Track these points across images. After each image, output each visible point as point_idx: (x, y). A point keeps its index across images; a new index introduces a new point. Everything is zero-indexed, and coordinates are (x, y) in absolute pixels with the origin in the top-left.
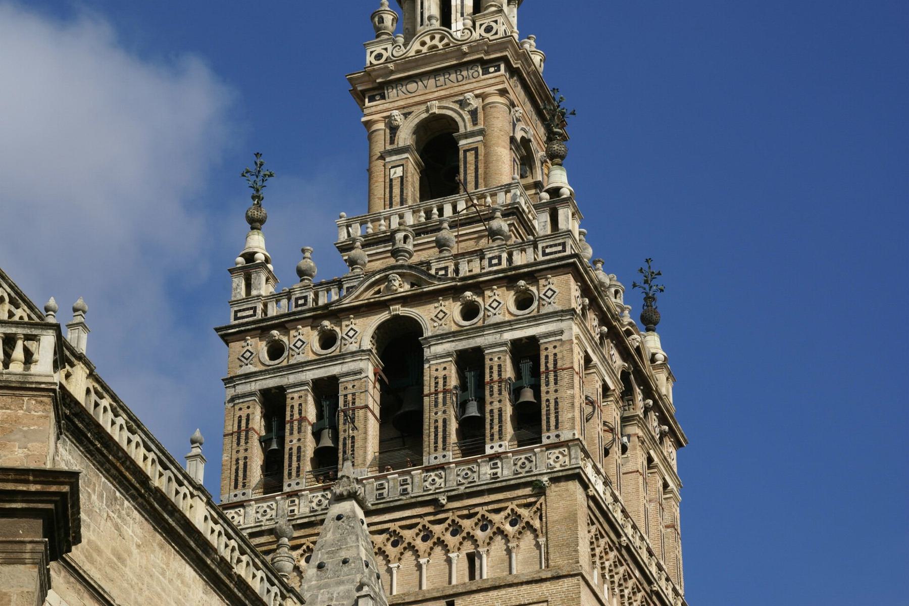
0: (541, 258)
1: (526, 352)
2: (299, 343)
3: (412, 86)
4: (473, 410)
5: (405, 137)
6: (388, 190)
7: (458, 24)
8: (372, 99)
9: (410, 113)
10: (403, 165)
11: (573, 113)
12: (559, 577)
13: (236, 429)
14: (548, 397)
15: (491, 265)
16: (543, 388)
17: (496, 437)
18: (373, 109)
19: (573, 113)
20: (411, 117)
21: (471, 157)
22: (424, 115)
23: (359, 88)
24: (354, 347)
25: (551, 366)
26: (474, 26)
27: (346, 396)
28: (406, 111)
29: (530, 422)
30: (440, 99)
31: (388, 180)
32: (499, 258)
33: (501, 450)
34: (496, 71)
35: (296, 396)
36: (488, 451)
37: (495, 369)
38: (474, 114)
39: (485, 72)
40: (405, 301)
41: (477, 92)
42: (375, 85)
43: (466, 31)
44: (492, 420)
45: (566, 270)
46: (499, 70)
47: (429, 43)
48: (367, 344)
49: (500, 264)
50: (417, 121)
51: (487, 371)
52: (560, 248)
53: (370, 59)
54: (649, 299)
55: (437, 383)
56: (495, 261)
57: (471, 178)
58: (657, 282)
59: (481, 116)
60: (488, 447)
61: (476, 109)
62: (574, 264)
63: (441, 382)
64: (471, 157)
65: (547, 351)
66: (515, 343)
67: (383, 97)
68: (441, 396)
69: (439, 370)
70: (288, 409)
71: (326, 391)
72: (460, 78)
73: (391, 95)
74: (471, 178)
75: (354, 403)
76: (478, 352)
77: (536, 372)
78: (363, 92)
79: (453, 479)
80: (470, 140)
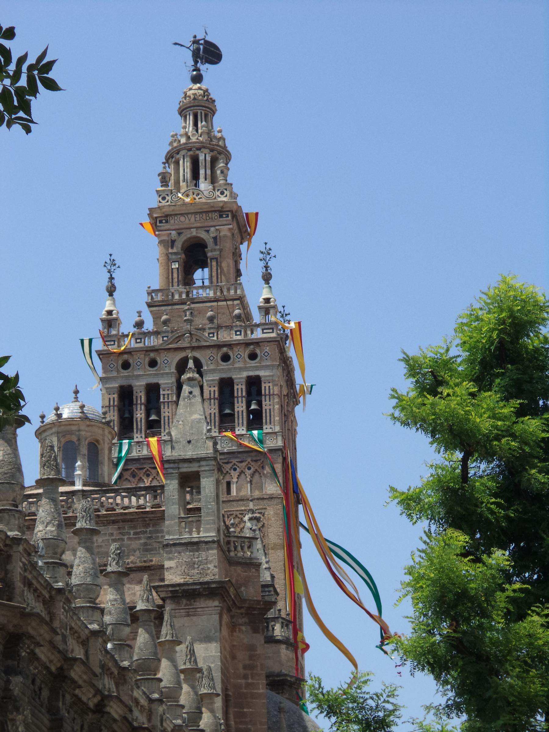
2: (139, 363)
3: (182, 219)
6: (170, 275)
7: (204, 185)
8: (161, 222)
9: (181, 233)
10: (178, 261)
11: (275, 257)
12: (272, 498)
13: (108, 404)
14: (266, 407)
15: (236, 335)
16: (264, 403)
17: (240, 425)
18: (162, 228)
19: (275, 257)
20: (182, 236)
22: (189, 236)
23: (155, 215)
25: (267, 392)
26: (214, 190)
27: (164, 395)
28: (179, 231)
29: (256, 420)
30: (197, 228)
31: (170, 269)
32: (240, 331)
33: (244, 432)
34: (226, 217)
35: (138, 391)
37: (240, 390)
38: (215, 238)
39: (221, 216)
40: (193, 348)
41: (217, 227)
42: (163, 215)
43: (211, 193)
44: (238, 416)
45: (274, 343)
46: (228, 216)
49: (240, 334)
50: (185, 238)
51: (236, 391)
52: (271, 331)
55: (210, 394)
56: (238, 333)
59: (218, 240)
60: (236, 430)
61: (216, 236)
62: (278, 341)
63: (212, 394)
66: (249, 378)
67: (167, 222)
68: (212, 401)
70: (134, 398)
72: (208, 218)
73: (172, 221)
75: (168, 399)
77: (259, 393)
78: (156, 218)
80: (214, 253)
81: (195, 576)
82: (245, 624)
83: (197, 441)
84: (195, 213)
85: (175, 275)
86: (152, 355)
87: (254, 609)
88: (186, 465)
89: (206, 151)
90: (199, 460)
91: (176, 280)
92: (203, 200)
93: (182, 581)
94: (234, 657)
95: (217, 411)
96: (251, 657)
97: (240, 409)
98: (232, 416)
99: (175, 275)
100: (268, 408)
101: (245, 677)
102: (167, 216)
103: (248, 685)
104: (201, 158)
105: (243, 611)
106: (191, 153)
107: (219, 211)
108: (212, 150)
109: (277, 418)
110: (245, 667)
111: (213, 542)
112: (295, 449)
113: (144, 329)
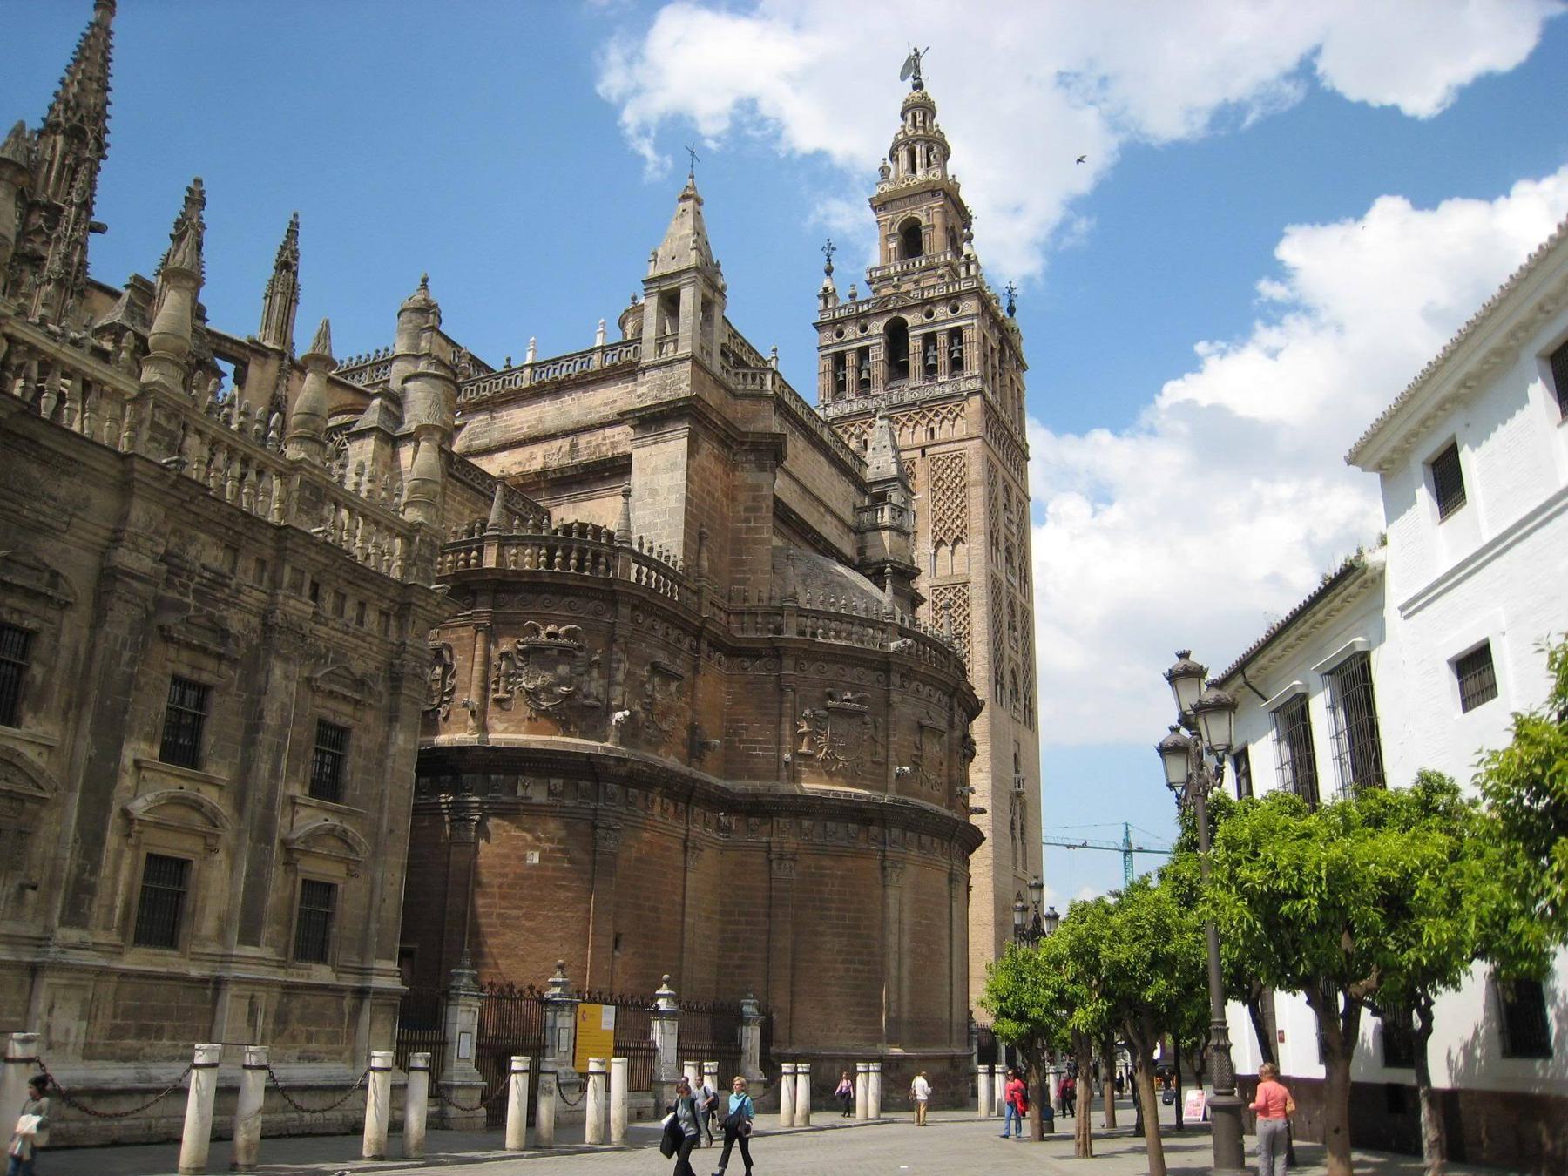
1: (956, 334)
4: (931, 362)
5: (896, 229)
7: (920, 172)
40: (899, 310)
54: (1011, 301)
65: (966, 333)
69: (915, 344)
71: (863, 353)
76: (934, 334)
77: (960, 343)
79: (924, 394)
94: (734, 499)
96: (754, 499)
101: (747, 520)
103: (749, 529)
110: (746, 510)
111: (686, 359)
112: (1021, 408)
113: (858, 299)
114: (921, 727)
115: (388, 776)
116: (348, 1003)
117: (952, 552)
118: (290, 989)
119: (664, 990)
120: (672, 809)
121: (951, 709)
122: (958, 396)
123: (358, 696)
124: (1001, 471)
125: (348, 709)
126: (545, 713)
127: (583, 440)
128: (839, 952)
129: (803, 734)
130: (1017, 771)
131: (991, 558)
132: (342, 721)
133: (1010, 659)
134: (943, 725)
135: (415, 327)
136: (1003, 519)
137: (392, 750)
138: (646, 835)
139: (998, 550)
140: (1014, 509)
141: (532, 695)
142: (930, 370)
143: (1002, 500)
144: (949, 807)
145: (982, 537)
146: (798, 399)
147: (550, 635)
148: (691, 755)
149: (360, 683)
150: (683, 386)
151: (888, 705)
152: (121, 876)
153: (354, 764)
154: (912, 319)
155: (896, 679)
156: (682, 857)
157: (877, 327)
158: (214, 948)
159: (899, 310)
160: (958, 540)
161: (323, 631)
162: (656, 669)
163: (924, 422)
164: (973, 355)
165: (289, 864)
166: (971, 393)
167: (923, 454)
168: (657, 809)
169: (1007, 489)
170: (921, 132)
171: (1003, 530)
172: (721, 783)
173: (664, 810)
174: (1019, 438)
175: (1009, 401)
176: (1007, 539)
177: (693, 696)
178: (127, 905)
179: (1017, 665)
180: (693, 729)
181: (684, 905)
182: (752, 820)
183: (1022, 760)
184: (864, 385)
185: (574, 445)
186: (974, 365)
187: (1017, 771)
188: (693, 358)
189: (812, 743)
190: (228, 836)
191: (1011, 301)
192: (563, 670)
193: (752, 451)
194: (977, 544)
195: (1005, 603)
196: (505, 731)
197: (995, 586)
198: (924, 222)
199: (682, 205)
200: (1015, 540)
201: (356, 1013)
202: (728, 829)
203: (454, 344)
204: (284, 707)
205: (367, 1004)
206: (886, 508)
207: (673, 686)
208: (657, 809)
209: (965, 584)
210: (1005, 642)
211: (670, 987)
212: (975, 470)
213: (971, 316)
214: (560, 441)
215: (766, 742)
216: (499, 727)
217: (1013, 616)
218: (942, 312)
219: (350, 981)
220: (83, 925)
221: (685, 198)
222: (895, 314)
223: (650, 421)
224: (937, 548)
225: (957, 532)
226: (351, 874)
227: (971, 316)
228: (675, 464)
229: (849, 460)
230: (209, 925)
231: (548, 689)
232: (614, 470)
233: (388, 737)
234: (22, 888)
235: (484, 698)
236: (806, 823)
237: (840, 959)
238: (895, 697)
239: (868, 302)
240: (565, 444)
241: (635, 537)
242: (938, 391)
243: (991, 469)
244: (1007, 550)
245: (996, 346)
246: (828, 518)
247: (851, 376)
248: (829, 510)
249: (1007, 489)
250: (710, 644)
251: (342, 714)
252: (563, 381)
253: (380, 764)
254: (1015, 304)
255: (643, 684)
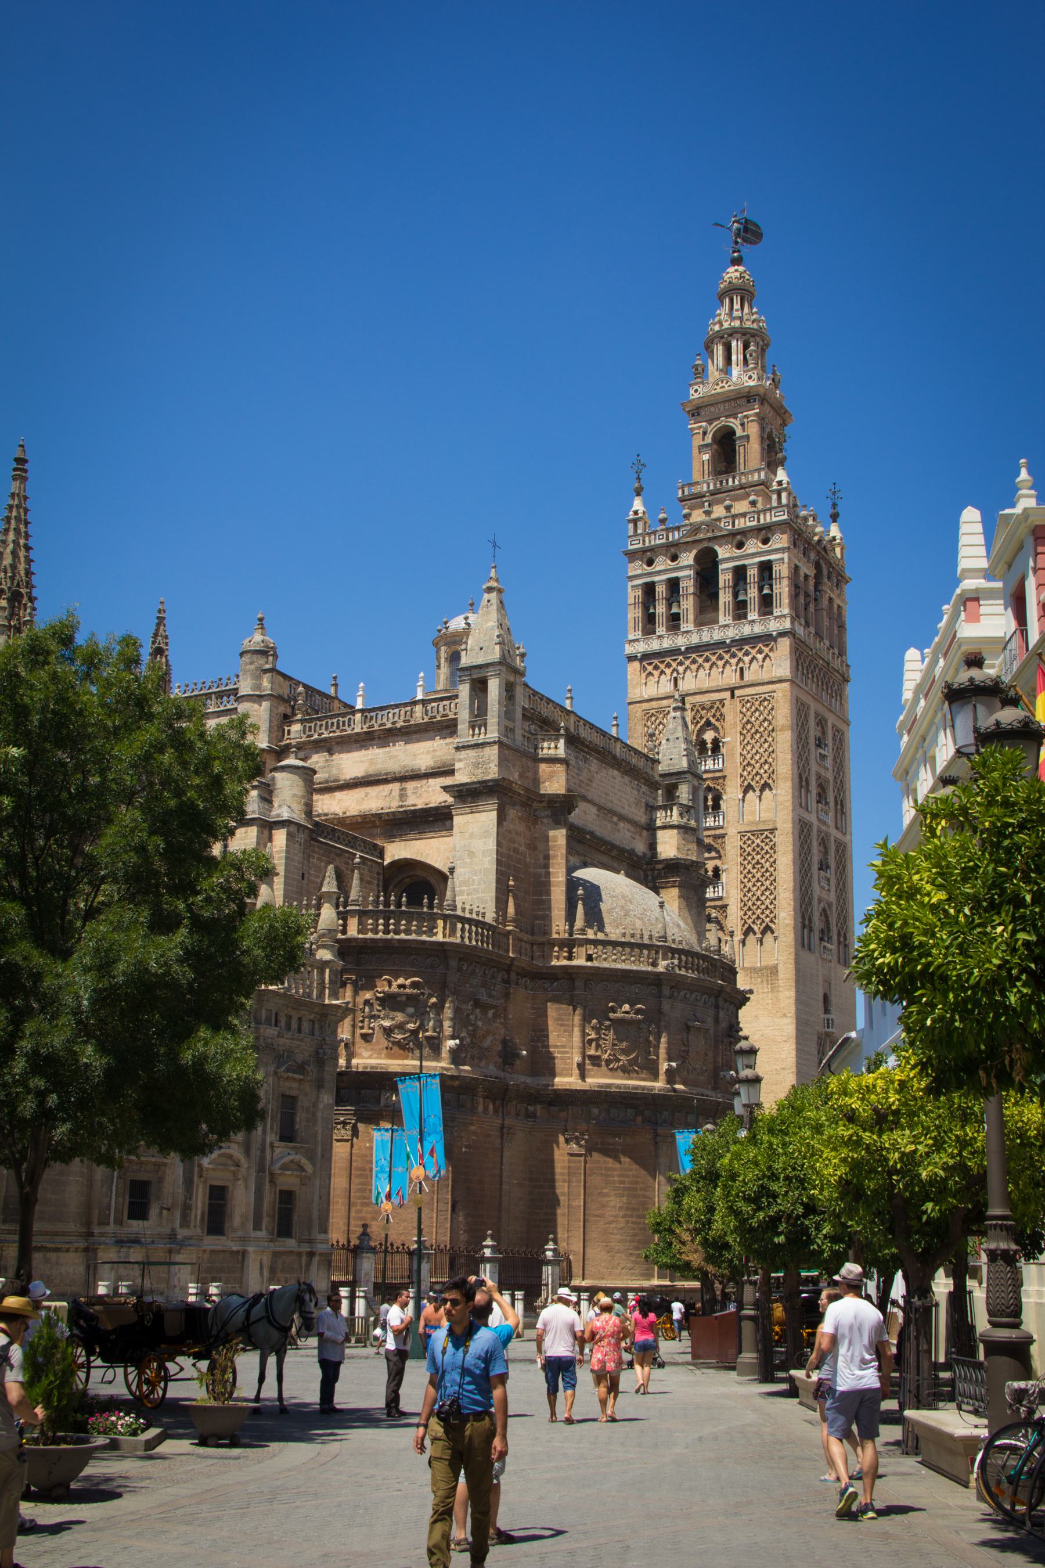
0: (774, 519)
3: (712, 409)
5: (709, 439)
21: (742, 450)
24: (686, 563)
36: (749, 618)
39: (749, 402)
47: (721, 385)
48: (691, 562)
53: (692, 392)
54: (834, 506)
57: (742, 461)
58: (838, 495)
64: (742, 450)
65: (776, 568)
66: (761, 563)
69: (725, 578)
74: (742, 461)
77: (771, 578)
81: (480, 776)
82: (548, 816)
83: (488, 648)
84: (724, 402)
85: (706, 467)
86: (672, 550)
87: (556, 802)
88: (477, 671)
89: (739, 335)
90: (487, 665)
91: (706, 472)
92: (732, 388)
93: (468, 781)
94: (535, 849)
95: (731, 599)
97: (752, 595)
98: (745, 602)
99: (706, 467)
100: (778, 591)
102: (698, 408)
104: (734, 344)
105: (544, 804)
106: (723, 340)
107: (747, 397)
108: (744, 334)
109: (787, 601)
111: (495, 742)
112: (842, 627)
114: (688, 1028)
115: (319, 1123)
116: (304, 1259)
117: (760, 797)
118: (276, 1255)
119: (489, 1242)
120: (491, 1107)
121: (717, 1007)
122: (767, 639)
123: (301, 1077)
124: (813, 706)
125: (295, 1085)
126: (397, 1044)
127: (410, 785)
128: (621, 1208)
129: (590, 1041)
130: (827, 1011)
131: (800, 802)
132: (294, 1093)
133: (820, 901)
134: (710, 1020)
135: (257, 669)
136: (814, 753)
137: (321, 1106)
138: (473, 1128)
139: (808, 791)
140: (829, 741)
141: (388, 1032)
142: (740, 609)
143: (813, 731)
144: (714, 1089)
145: (789, 784)
146: (592, 726)
147: (400, 986)
148: (505, 1063)
149: (301, 1068)
150: (492, 765)
151: (660, 1012)
152: (200, 1201)
153: (300, 1118)
154: (723, 552)
155: (666, 991)
156: (499, 1141)
157: (688, 558)
158: (240, 1234)
159: (710, 539)
160: (766, 786)
161: (281, 1041)
162: (477, 1004)
163: (734, 661)
164: (782, 590)
165: (272, 1181)
166: (782, 634)
167: (733, 696)
168: (481, 1108)
169: (821, 722)
170: (737, 324)
171: (814, 767)
172: (529, 1080)
173: (486, 1109)
174: (836, 664)
175: (826, 622)
176: (819, 776)
177: (506, 1017)
178: (203, 1214)
179: (830, 905)
180: (505, 1042)
181: (501, 1176)
182: (552, 1108)
183: (834, 1000)
184: (674, 621)
185: (403, 790)
186: (783, 607)
187: (827, 1011)
188: (500, 743)
189: (598, 1046)
190: (243, 1171)
191: (834, 506)
192: (411, 1010)
193: (549, 807)
194: (784, 790)
195: (815, 844)
196: (370, 1057)
197: (803, 831)
198: (739, 432)
199: (486, 596)
200: (830, 775)
201: (308, 1265)
202: (533, 1115)
203: (290, 679)
204: (266, 1091)
205: (316, 1259)
206: (675, 808)
207: (490, 1013)
208: (481, 1108)
209: (772, 831)
210: (815, 886)
211: (493, 1239)
212: (783, 713)
213: (781, 550)
214: (391, 786)
215: (563, 1046)
216: (366, 1054)
217: (826, 852)
218: (753, 546)
219: (305, 1248)
220: (188, 1227)
221: (490, 590)
222: (705, 544)
223: (469, 795)
224: (745, 792)
225: (765, 776)
226: (303, 1184)
227: (781, 550)
228: (486, 831)
229: (641, 763)
230: (237, 1221)
231: (401, 1027)
232: (435, 820)
233: (318, 1098)
234: (162, 1208)
235: (353, 1033)
236: (595, 1111)
237: (622, 1213)
238: (666, 1006)
239: (678, 528)
240: (396, 786)
241: (459, 905)
242: (747, 630)
243: (800, 711)
244: (822, 788)
245: (811, 572)
246: (621, 824)
247: (661, 609)
248: (622, 818)
249: (821, 722)
250: (518, 974)
251: (291, 1087)
252: (390, 730)
253: (314, 1114)
254: (839, 509)
255: (468, 1015)
